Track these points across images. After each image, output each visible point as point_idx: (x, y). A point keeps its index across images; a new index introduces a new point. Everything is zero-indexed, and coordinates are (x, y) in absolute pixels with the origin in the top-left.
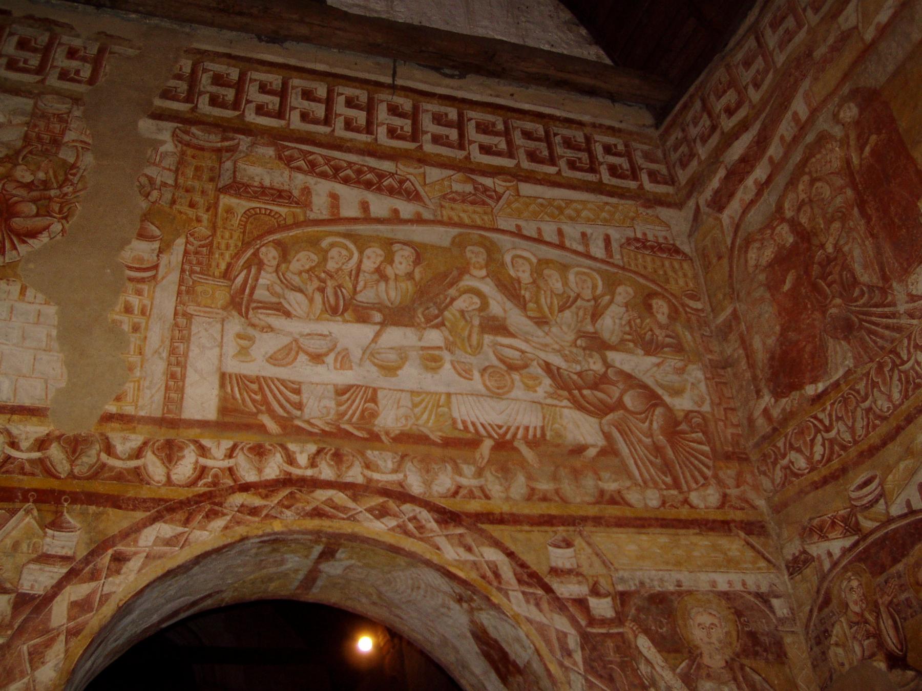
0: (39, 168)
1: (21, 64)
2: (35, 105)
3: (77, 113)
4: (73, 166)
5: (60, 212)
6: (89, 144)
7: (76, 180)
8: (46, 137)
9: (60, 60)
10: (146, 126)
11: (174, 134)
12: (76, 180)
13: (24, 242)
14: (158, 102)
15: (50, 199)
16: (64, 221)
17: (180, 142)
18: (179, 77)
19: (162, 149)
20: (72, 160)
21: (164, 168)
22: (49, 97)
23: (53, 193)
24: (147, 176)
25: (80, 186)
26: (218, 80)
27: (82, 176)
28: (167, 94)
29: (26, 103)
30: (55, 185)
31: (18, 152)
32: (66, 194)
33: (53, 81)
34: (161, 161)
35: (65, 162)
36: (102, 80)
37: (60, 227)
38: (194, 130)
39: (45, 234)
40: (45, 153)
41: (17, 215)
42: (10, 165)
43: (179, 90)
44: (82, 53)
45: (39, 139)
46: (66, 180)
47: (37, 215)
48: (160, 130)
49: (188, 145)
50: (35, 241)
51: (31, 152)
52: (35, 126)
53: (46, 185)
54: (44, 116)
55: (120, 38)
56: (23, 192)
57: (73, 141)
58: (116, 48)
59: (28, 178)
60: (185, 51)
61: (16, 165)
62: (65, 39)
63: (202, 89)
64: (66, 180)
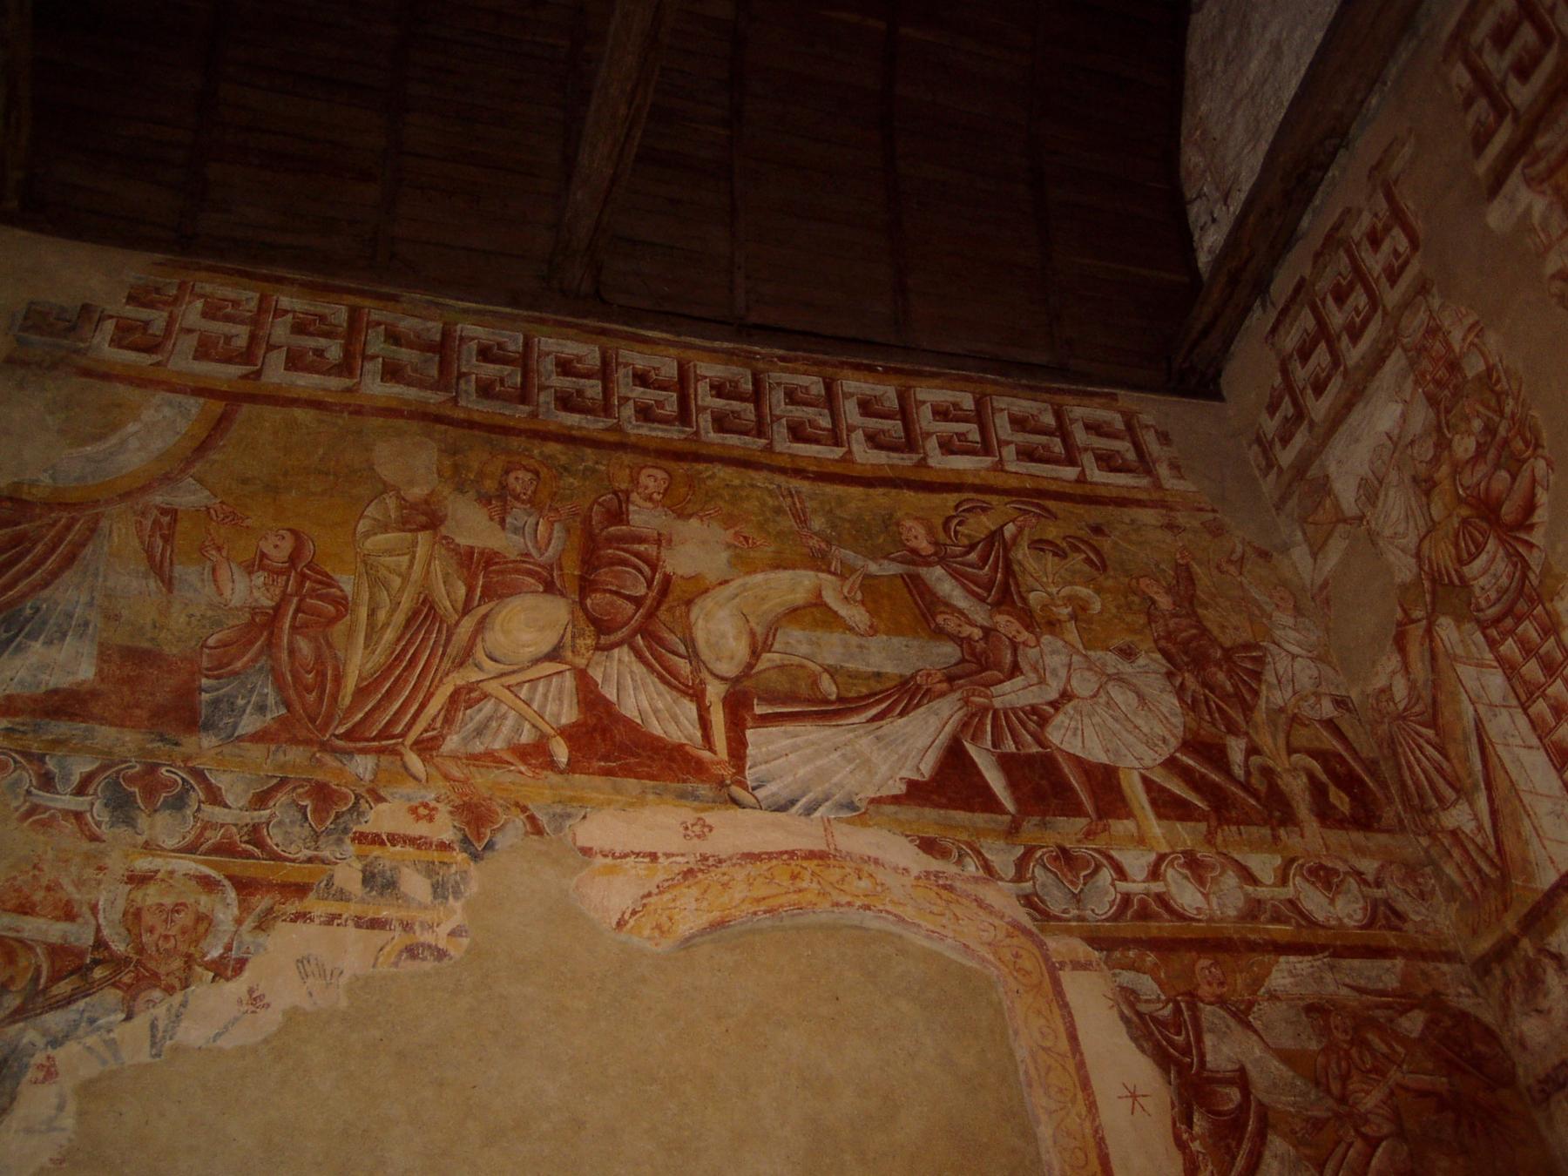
0: (1468, 420)
1: (1358, 320)
2: (1405, 350)
3: (1436, 303)
4: (1490, 370)
5: (1527, 446)
6: (1477, 322)
7: (1504, 385)
8: (1442, 373)
9: (1375, 263)
10: (1497, 216)
11: (1529, 182)
12: (1504, 385)
13: (1531, 527)
14: (1481, 168)
15: (1506, 442)
16: (1540, 451)
17: (1542, 181)
18: (1469, 103)
19: (1536, 217)
20: (1482, 367)
21: (1560, 238)
22: (1404, 323)
23: (1502, 431)
24: (1553, 277)
25: (1515, 387)
26: (1502, 37)
27: (1506, 373)
28: (1480, 142)
29: (1396, 361)
30: (1497, 419)
31: (1439, 429)
32: (1513, 415)
33: (1392, 297)
34: (1549, 236)
35: (1478, 378)
36: (1419, 226)
37: (1541, 464)
38: (1541, 142)
39: (1539, 490)
40: (1457, 393)
41: (1500, 505)
42: (1446, 453)
43: (1482, 119)
44: (1379, 226)
45: (1439, 383)
46: (1498, 395)
47: (1514, 478)
48: (1512, 200)
49: (1551, 171)
50: (1539, 512)
51: (1448, 411)
52: (1423, 375)
53: (1489, 430)
54: (1422, 350)
55: (1386, 151)
56: (1482, 469)
57: (1464, 339)
58: (1396, 167)
59: (1471, 444)
60: (1444, 61)
61: (1449, 445)
62: (1356, 233)
63: (1498, 77)
64: (1498, 395)
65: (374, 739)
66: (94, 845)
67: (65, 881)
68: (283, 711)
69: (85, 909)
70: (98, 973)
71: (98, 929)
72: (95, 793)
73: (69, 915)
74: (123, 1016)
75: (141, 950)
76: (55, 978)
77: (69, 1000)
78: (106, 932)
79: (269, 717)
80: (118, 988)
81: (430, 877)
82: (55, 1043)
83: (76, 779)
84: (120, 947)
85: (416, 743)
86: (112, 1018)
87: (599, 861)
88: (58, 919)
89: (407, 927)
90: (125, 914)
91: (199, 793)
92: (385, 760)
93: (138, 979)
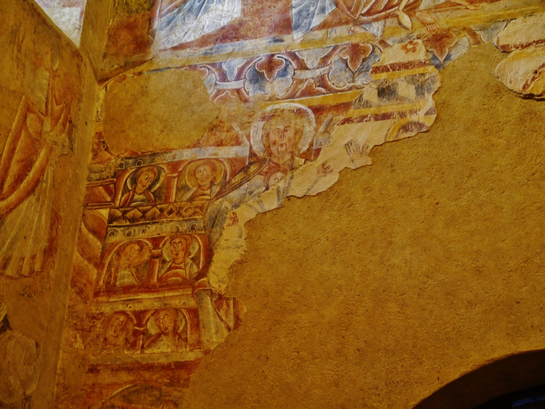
65: (382, 11)
66: (247, 105)
67: (235, 125)
68: (334, 7)
69: (245, 138)
70: (253, 168)
71: (251, 148)
72: (245, 78)
73: (238, 143)
74: (264, 188)
75: (270, 154)
76: (234, 175)
77: (240, 184)
78: (254, 148)
79: (327, 13)
80: (261, 175)
81: (414, 84)
82: (236, 206)
83: (236, 72)
84: (261, 155)
85: (406, 7)
86: (260, 190)
87: (515, 52)
88: (233, 145)
89: (402, 115)
90: (262, 137)
91: (294, 65)
92: (389, 21)
93: (270, 168)
